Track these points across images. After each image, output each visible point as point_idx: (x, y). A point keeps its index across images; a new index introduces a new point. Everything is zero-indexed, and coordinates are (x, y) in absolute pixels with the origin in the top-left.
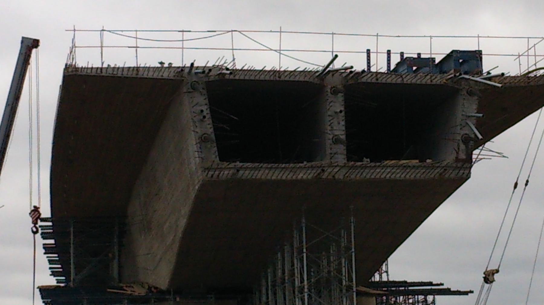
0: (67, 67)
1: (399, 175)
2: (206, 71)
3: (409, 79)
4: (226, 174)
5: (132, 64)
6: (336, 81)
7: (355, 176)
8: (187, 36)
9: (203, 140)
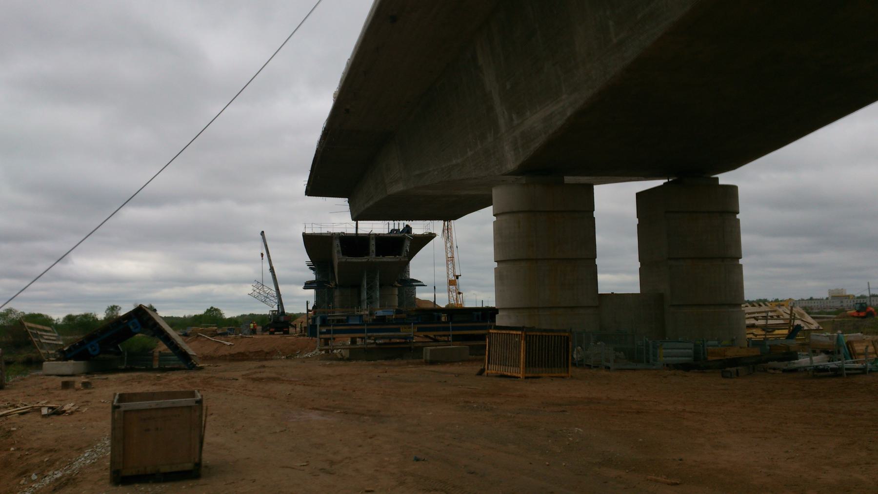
0: (303, 233)
1: (390, 260)
2: (339, 234)
3: (392, 235)
4: (343, 260)
5: (320, 232)
6: (373, 236)
7: (377, 260)
8: (334, 224)
9: (338, 252)
